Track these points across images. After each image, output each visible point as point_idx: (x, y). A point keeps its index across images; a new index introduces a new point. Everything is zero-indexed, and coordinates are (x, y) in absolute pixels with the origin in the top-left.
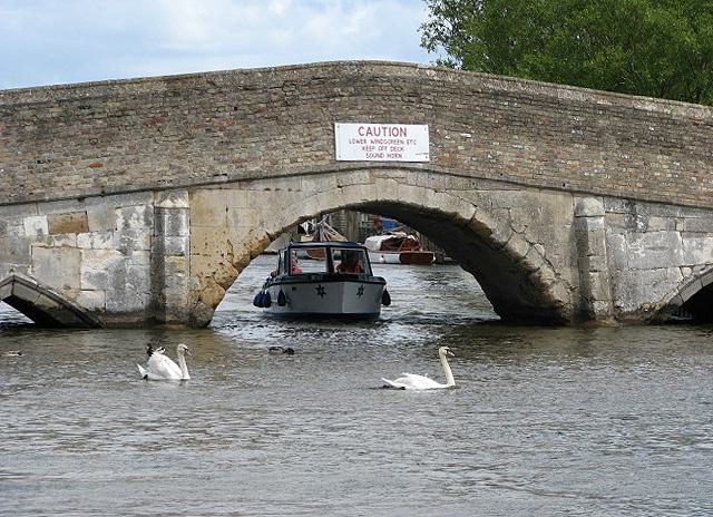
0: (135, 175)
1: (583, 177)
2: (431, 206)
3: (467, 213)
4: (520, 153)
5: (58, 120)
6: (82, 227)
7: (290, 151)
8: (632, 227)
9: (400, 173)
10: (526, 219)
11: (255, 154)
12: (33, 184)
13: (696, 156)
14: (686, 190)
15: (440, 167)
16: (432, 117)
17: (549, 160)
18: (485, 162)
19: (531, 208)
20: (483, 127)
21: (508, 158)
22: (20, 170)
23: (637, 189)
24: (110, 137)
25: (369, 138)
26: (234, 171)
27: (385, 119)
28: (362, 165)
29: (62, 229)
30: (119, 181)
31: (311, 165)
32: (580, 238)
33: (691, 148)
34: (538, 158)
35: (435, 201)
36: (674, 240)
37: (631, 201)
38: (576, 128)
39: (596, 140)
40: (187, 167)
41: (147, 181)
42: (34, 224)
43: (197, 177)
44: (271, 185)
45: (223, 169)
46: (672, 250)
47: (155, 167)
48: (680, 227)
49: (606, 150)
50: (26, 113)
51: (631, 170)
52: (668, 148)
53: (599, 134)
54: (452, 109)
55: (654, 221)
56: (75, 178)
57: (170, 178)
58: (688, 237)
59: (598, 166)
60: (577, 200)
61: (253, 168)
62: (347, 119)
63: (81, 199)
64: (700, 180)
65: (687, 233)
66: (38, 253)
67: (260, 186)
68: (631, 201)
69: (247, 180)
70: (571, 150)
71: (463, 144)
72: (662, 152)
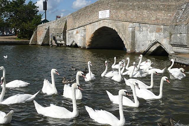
1: (131, 18)
2: (109, 27)
3: (114, 28)
4: (121, 13)
8: (140, 30)
10: (122, 29)
13: (152, 9)
14: (149, 20)
15: (111, 18)
17: (126, 15)
18: (116, 16)
19: (123, 26)
20: (117, 9)
23: (140, 20)
25: (103, 13)
28: (101, 19)
31: (96, 20)
32: (133, 33)
33: (151, 7)
34: (124, 15)
35: (110, 26)
36: (147, 34)
38: (131, 6)
40: (86, 22)
45: (88, 22)
46: (147, 36)
47: (83, 23)
48: (149, 30)
49: (135, 11)
51: (139, 15)
52: (146, 8)
53: (134, 7)
55: (144, 29)
58: (150, 33)
62: (100, 10)
63: (78, 28)
64: (152, 16)
65: (151, 32)
70: (129, 12)
72: (145, 10)
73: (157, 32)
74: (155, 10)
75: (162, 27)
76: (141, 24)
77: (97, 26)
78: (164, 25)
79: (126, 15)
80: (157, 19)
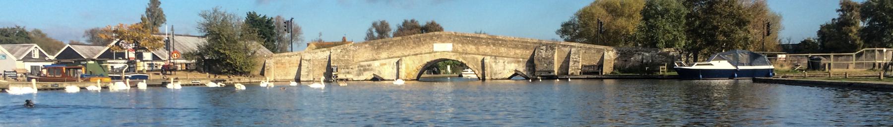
0: (395, 55)
3: (460, 60)
5: (381, 45)
6: (385, 64)
7: (425, 49)
9: (446, 53)
11: (418, 50)
12: (376, 57)
13: (510, 47)
15: (455, 51)
16: (454, 41)
17: (478, 49)
18: (463, 50)
19: (474, 59)
21: (469, 50)
22: (375, 55)
24: (390, 48)
26: (414, 53)
27: (443, 42)
29: (382, 65)
30: (392, 56)
37: (495, 57)
39: (488, 44)
41: (397, 55)
42: (376, 64)
43: (406, 54)
44: (421, 55)
48: (506, 62)
50: (376, 45)
54: (457, 40)
55: (501, 61)
56: (384, 55)
57: (401, 55)
59: (488, 50)
60: (484, 56)
61: (417, 53)
66: (377, 69)
67: (419, 56)
68: (495, 57)
69: (416, 55)
71: (460, 47)
73: (515, 63)
74: (513, 48)
75: (521, 60)
76: (497, 58)
77: (428, 59)
78: (523, 58)
79: (478, 49)
80: (515, 54)
